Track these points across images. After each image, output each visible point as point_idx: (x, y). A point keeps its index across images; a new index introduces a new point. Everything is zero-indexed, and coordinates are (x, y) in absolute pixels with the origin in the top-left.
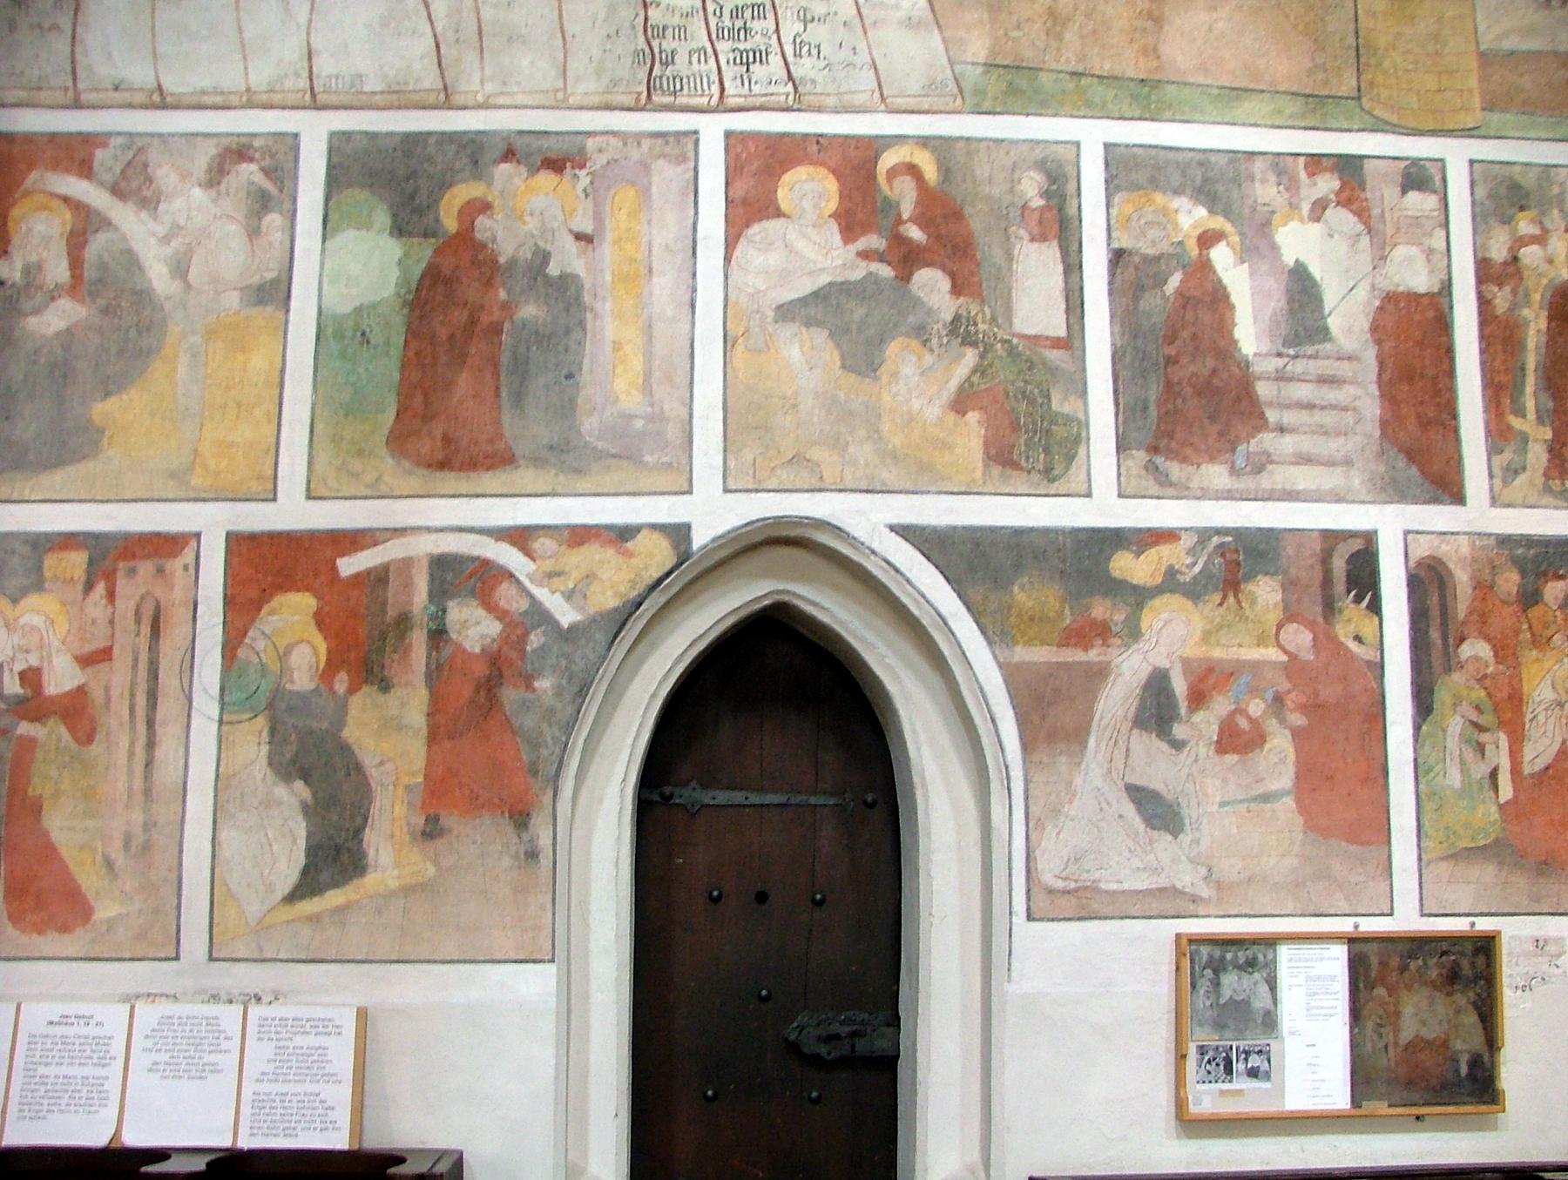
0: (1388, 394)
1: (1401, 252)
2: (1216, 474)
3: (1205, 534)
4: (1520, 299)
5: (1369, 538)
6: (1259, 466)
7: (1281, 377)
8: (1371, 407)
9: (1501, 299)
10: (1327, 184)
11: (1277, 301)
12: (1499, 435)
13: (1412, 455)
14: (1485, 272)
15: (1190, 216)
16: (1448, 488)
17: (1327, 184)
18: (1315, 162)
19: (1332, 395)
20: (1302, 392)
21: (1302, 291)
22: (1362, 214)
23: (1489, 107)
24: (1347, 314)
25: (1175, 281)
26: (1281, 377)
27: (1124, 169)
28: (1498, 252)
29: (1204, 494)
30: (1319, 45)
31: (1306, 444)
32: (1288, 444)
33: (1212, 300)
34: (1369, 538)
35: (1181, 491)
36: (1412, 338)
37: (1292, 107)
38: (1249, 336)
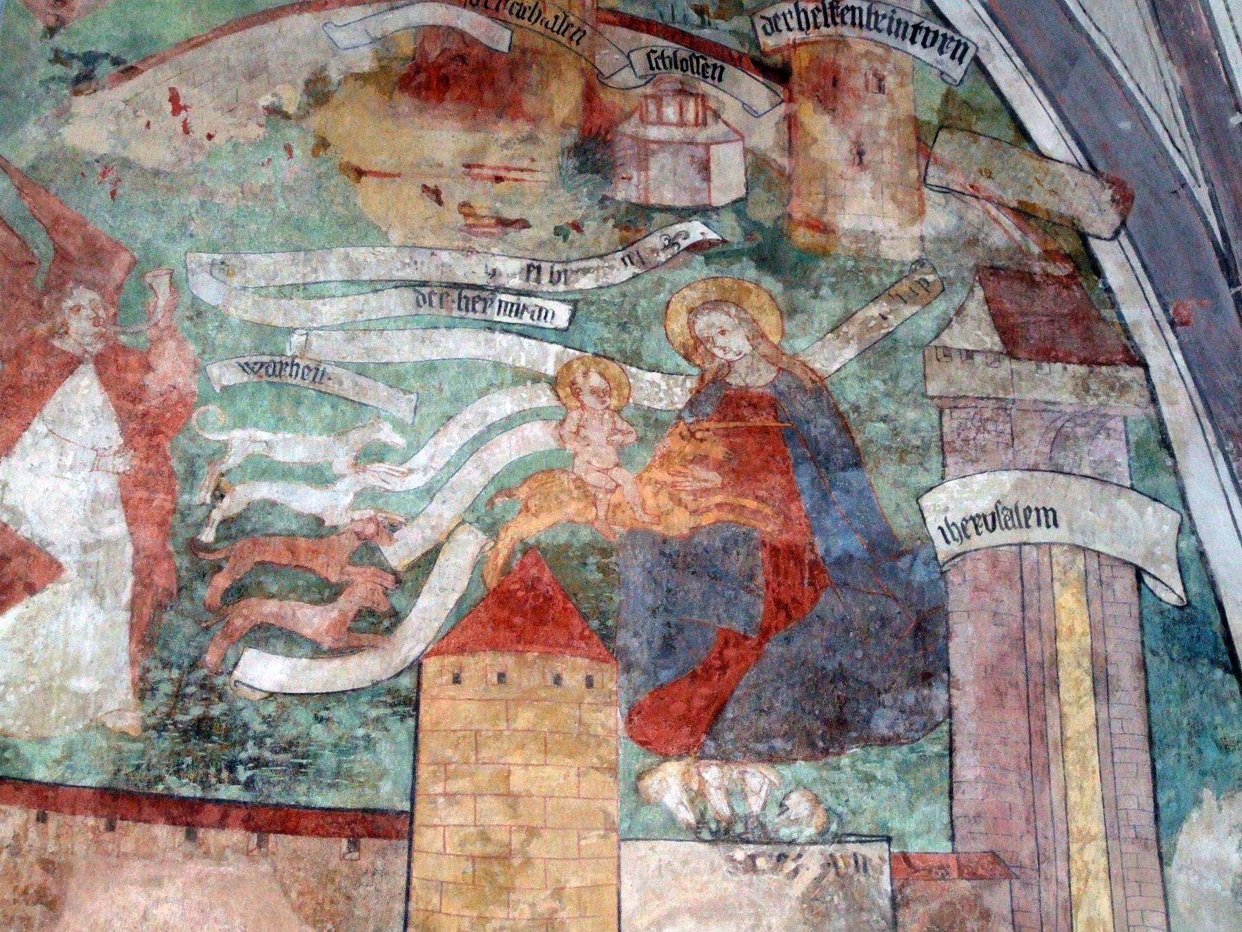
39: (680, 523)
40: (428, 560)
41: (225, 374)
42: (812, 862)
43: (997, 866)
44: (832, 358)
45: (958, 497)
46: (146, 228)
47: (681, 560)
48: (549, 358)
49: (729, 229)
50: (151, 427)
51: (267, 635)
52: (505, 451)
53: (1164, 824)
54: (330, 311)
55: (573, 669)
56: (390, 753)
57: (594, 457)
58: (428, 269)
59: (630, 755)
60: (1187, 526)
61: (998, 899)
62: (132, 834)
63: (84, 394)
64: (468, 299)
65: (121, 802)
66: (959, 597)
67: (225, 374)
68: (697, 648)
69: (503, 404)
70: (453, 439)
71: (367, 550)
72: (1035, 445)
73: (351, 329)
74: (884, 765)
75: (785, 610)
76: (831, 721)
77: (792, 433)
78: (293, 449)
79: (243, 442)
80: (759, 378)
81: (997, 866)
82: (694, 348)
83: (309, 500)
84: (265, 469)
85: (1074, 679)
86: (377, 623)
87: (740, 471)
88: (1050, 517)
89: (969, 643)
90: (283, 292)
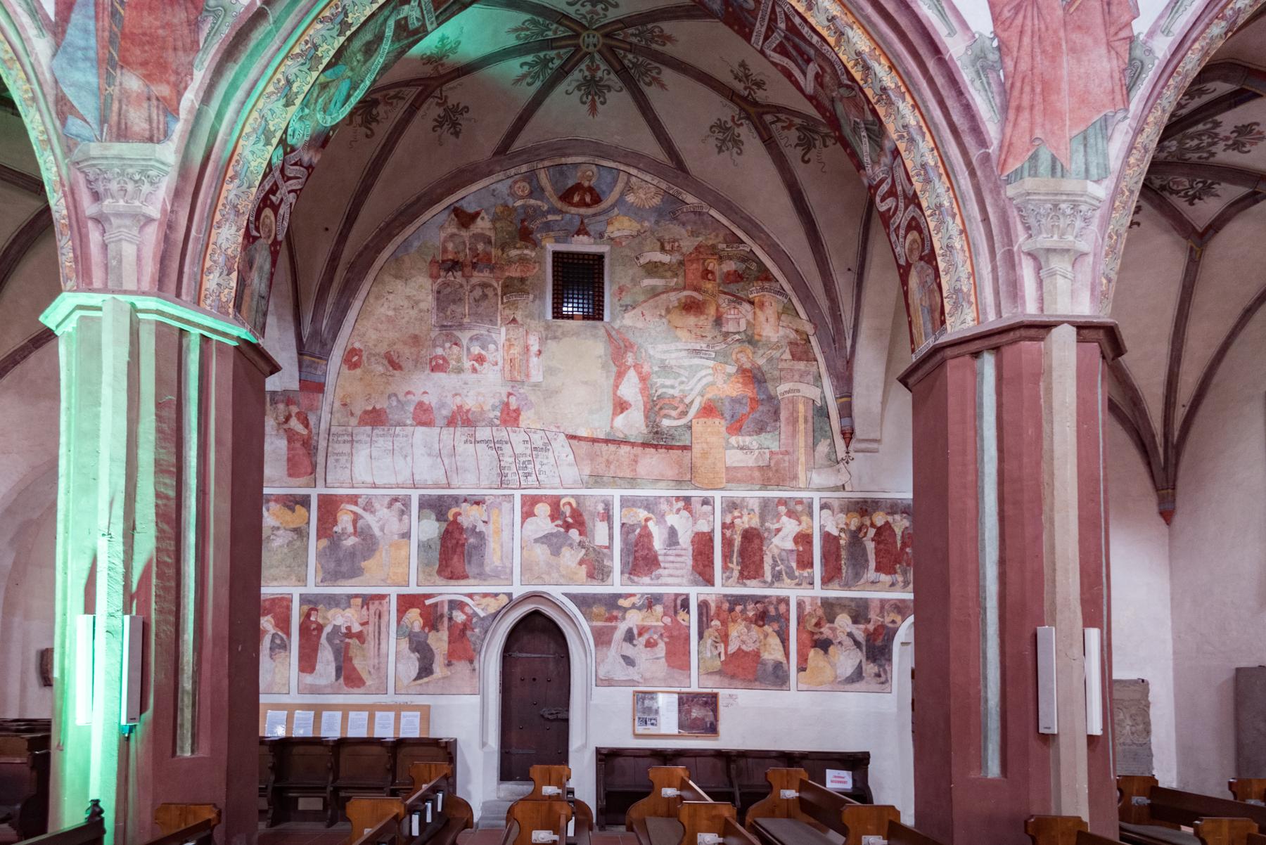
0: (695, 559)
1: (700, 522)
2: (646, 580)
3: (643, 595)
4: (734, 532)
5: (687, 595)
6: (658, 577)
7: (665, 555)
8: (690, 562)
9: (728, 533)
10: (681, 504)
11: (666, 535)
12: (725, 568)
13: (700, 574)
14: (724, 526)
15: (643, 514)
16: (710, 582)
17: (681, 504)
18: (678, 498)
19: (679, 559)
20: (671, 558)
21: (673, 532)
22: (690, 512)
23: (728, 482)
24: (685, 539)
25: (638, 531)
26: (665, 555)
27: (626, 503)
28: (728, 521)
29: (643, 585)
30: (681, 467)
31: (671, 572)
32: (666, 572)
33: (647, 535)
34: (687, 595)
35: (637, 584)
36: (703, 545)
37: (673, 484)
38: (658, 544)
39: (734, 394)
40: (692, 402)
41: (656, 369)
42: (757, 452)
43: (787, 453)
44: (761, 362)
45: (782, 388)
46: (640, 341)
47: (735, 401)
48: (711, 363)
49: (743, 336)
50: (643, 379)
51: (666, 416)
52: (704, 381)
53: (815, 445)
54: (673, 355)
55: (717, 421)
56: (687, 436)
57: (720, 383)
58: (689, 347)
59: (727, 435)
60: (823, 392)
61: (786, 458)
62: (647, 450)
63: (632, 374)
64: (697, 352)
65: (645, 445)
66: (782, 406)
67: (656, 369)
68: (738, 416)
69: (703, 373)
70: (695, 380)
71: (682, 401)
72: (797, 377)
73: (676, 359)
74: (769, 436)
75: (752, 409)
76: (761, 429)
77: (754, 377)
78: (668, 382)
79: (659, 381)
80: (748, 366)
81: (787, 453)
82: (737, 360)
83: (671, 391)
84: (664, 386)
85: (801, 420)
86: (684, 413)
87: (745, 384)
88: (798, 391)
89: (784, 414)
90: (665, 352)
